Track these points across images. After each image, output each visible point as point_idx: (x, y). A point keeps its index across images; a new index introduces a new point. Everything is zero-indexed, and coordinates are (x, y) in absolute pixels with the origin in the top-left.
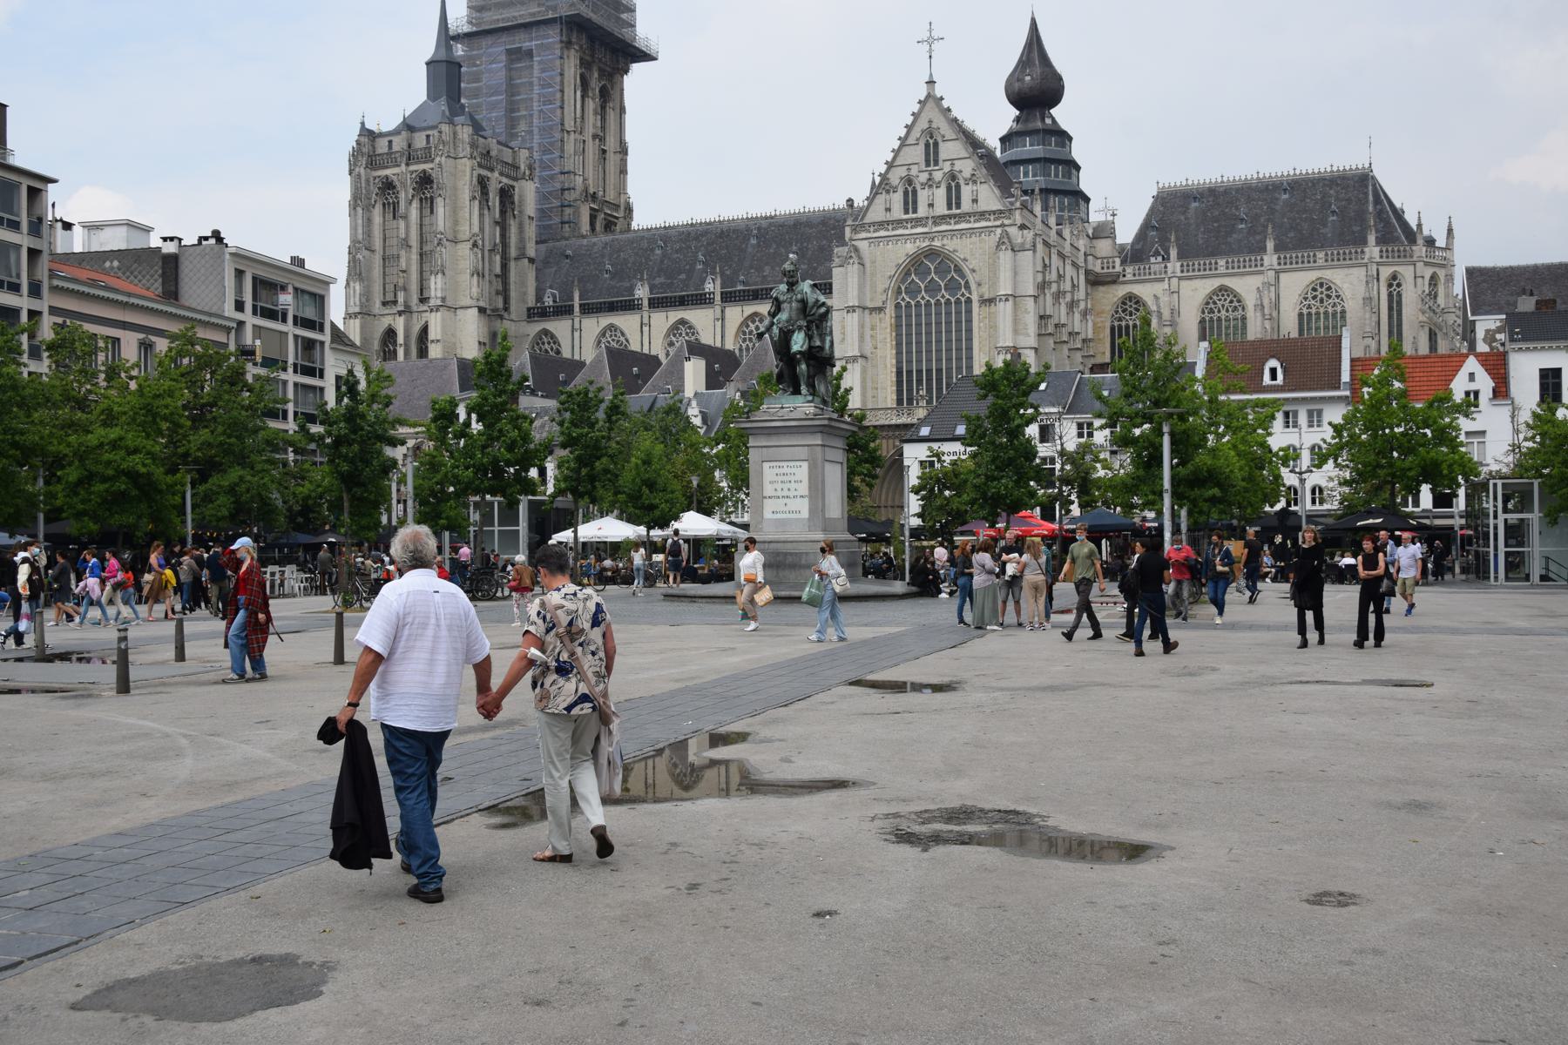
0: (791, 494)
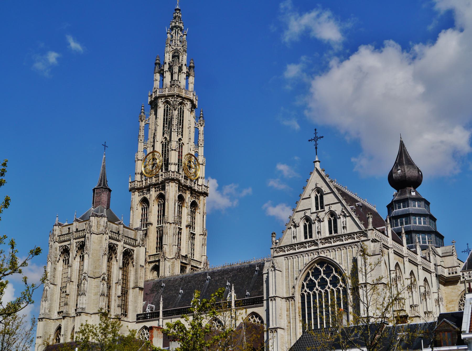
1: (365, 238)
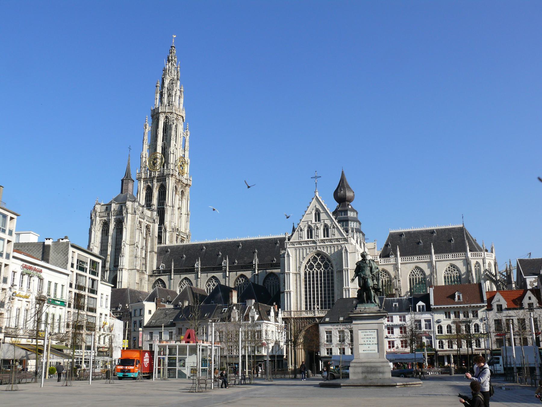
0: (371, 343)
1: (346, 243)
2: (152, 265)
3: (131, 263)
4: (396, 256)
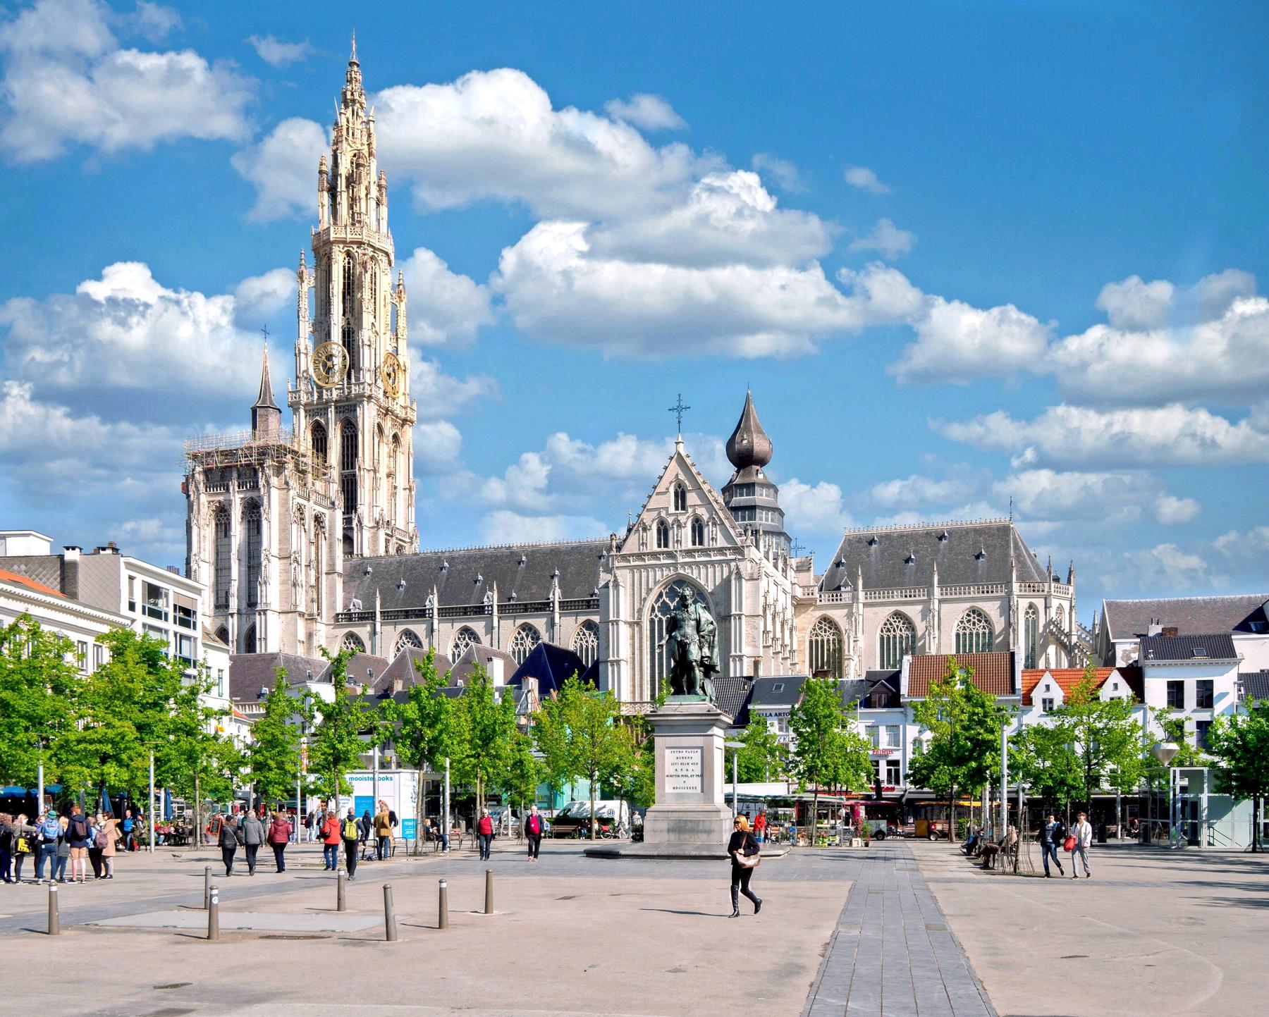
2: (332, 604)
3: (285, 596)
4: (856, 589)
